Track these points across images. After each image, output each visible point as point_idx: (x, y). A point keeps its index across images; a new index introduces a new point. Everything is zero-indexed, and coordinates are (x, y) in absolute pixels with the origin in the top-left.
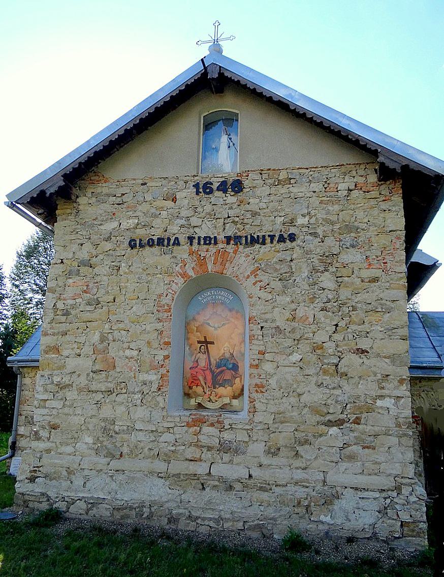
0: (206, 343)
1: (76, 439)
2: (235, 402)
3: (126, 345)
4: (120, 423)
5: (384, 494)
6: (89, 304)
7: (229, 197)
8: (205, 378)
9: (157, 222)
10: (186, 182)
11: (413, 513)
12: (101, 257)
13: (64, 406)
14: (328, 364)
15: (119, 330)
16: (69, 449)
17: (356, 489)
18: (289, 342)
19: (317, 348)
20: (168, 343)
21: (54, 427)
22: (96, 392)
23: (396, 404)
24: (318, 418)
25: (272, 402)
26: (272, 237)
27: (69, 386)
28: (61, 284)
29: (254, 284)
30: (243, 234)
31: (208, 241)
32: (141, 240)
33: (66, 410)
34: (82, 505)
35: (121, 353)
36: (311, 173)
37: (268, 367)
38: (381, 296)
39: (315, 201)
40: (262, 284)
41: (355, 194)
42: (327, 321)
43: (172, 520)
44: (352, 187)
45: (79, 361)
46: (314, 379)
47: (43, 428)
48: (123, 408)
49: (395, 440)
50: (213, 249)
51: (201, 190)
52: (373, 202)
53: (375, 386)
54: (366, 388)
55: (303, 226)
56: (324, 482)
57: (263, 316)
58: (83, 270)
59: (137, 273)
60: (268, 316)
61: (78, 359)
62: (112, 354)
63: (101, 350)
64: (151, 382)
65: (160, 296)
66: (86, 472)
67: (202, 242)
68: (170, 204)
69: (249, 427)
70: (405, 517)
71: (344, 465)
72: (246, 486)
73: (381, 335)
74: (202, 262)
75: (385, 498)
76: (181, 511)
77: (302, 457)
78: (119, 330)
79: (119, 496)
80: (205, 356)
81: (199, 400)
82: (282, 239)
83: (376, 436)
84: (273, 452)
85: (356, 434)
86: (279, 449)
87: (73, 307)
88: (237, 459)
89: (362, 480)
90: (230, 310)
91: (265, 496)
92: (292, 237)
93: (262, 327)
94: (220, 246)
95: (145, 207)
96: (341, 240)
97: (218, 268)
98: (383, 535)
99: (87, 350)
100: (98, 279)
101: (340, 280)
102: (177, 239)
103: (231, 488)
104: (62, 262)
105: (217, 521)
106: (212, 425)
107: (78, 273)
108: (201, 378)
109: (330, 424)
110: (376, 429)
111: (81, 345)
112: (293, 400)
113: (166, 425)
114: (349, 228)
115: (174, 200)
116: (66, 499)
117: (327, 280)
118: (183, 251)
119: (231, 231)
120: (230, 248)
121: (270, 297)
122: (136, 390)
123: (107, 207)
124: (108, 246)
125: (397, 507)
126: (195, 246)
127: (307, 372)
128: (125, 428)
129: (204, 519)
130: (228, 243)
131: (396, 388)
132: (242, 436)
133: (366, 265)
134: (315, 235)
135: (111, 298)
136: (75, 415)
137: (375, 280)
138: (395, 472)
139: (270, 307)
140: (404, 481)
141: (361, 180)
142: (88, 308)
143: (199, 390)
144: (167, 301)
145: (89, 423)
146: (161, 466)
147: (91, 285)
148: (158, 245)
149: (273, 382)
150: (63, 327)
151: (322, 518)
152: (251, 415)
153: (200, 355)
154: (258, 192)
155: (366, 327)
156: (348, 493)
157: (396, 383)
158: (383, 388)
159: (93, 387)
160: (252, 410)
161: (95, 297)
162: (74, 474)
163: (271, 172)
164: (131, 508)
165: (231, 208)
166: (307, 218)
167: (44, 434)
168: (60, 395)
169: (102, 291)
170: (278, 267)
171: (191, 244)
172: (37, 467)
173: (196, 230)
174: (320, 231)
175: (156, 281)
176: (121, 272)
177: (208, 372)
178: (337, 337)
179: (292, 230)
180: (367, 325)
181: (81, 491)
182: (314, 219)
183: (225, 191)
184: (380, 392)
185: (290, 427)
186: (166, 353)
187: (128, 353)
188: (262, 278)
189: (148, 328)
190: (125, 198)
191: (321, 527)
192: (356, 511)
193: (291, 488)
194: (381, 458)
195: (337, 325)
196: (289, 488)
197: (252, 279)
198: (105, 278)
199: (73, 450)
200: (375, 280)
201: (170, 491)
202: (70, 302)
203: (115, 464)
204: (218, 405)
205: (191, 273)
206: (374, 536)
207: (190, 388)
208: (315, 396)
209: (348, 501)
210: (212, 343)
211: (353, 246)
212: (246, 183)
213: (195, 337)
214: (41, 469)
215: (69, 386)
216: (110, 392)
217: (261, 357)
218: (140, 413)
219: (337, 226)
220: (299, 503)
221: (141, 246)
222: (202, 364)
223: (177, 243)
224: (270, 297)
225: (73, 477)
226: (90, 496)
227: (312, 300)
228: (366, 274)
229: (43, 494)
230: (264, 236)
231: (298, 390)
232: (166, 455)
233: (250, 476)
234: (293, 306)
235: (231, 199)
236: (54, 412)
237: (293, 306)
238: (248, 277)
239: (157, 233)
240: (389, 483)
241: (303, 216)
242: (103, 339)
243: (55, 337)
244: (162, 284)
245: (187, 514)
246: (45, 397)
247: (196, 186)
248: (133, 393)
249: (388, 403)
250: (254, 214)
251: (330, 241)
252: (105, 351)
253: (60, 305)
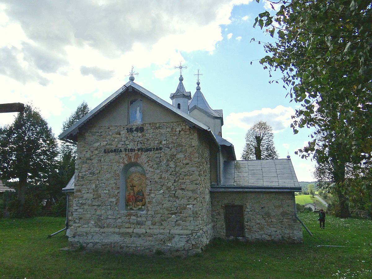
0: (133, 186)
1: (89, 223)
2: (143, 207)
3: (104, 189)
4: (103, 216)
5: (188, 236)
6: (90, 174)
7: (139, 133)
8: (133, 199)
9: (114, 143)
10: (124, 127)
11: (196, 241)
12: (94, 156)
13: (84, 211)
14: (172, 194)
15: (101, 183)
16: (86, 226)
17: (179, 235)
18: (160, 186)
19: (168, 188)
20: (118, 188)
21: (81, 218)
22: (94, 206)
23: (193, 207)
24: (169, 212)
25: (153, 207)
26: (154, 148)
27: (85, 204)
28: (80, 167)
29: (148, 166)
30: (144, 147)
31: (132, 150)
32: (108, 150)
33: (84, 212)
34: (91, 244)
35: (103, 192)
36: (167, 124)
37: (153, 195)
38: (189, 170)
39: (168, 135)
40: (151, 166)
41: (182, 132)
42: (172, 179)
43: (122, 248)
44: (181, 130)
45: (88, 195)
46: (167, 199)
47: (77, 219)
48: (104, 211)
49: (192, 218)
50: (133, 153)
51: (129, 131)
52: (188, 136)
53: (186, 201)
54: (184, 201)
55: (164, 144)
56: (169, 233)
57: (151, 177)
58: (88, 161)
59: (107, 162)
60: (153, 177)
61: (88, 194)
62: (100, 191)
63: (96, 190)
64: (113, 202)
65: (115, 170)
66: (92, 234)
67: (130, 151)
68: (118, 136)
69: (146, 216)
70: (194, 243)
71: (176, 227)
72: (145, 236)
73: (189, 183)
74: (130, 158)
75: (188, 237)
76: (124, 245)
77: (163, 225)
78: (101, 183)
79: (104, 241)
80: (133, 191)
81: (131, 207)
82: (157, 149)
83: (186, 217)
84: (154, 224)
85: (180, 217)
86: (156, 223)
87: (85, 175)
88: (143, 227)
89: (182, 232)
90: (141, 174)
91: (151, 238)
92: (161, 149)
93: (151, 181)
94: (136, 152)
95: (109, 137)
96: (177, 150)
97: (135, 160)
98: (187, 249)
99: (91, 191)
100: (93, 165)
101: (176, 164)
102: (121, 149)
103: (140, 236)
104: (80, 158)
105: (136, 247)
106: (134, 216)
107: (86, 163)
108: (131, 199)
109: (172, 214)
110: (186, 215)
111: (88, 189)
112: (160, 206)
113: (119, 216)
114: (180, 145)
115: (120, 134)
116: (86, 243)
117: (172, 165)
118: (123, 155)
119: (140, 146)
120: (139, 153)
121: (153, 170)
122: (108, 204)
123: (95, 137)
124: (96, 152)
125: (192, 240)
126: (127, 153)
127: (165, 196)
128: (105, 218)
129: (132, 247)
130: (139, 151)
131: (193, 201)
132: (144, 219)
133: (185, 159)
134: (168, 148)
135: (98, 171)
136: (88, 214)
137: (187, 164)
138: (192, 229)
139: (153, 174)
140: (194, 231)
141: (184, 127)
142: (91, 175)
143: (131, 203)
144: (119, 173)
145: (92, 217)
146: (117, 230)
147: (91, 167)
148: (114, 152)
149: (154, 200)
150: (82, 183)
151: (168, 244)
152: (147, 212)
153: (131, 191)
154: (149, 131)
155: (184, 181)
156: (177, 236)
157: (193, 200)
158: (189, 201)
159: (94, 203)
160: (147, 210)
161: (93, 171)
162: (88, 234)
163: (154, 124)
164: (108, 245)
165: (139, 138)
166: (166, 141)
167: (77, 221)
168: (82, 207)
169: (95, 169)
170: (156, 159)
171: (126, 152)
172: (76, 232)
173: (128, 146)
174: (170, 146)
175: (114, 165)
176: (102, 162)
177: (133, 197)
178: (175, 184)
179: (161, 146)
180: (184, 180)
181: (91, 240)
182: (168, 142)
183: (137, 132)
184: (188, 203)
185: (160, 215)
186: (118, 191)
187: (105, 191)
188: (151, 164)
189: (112, 182)
190: (102, 134)
191: (168, 247)
192: (179, 242)
193: (159, 236)
194: (188, 224)
195: (175, 180)
196: (158, 235)
197: (147, 164)
198: (96, 164)
199: (88, 226)
200: (187, 164)
201: (120, 238)
202: (84, 173)
203: (102, 230)
204: (137, 208)
205: (126, 162)
206: (184, 249)
207: (128, 203)
208: (167, 204)
209: (177, 239)
210: (135, 186)
211: (181, 152)
212: (145, 128)
213: (129, 184)
214: (77, 233)
215: (85, 204)
216: (99, 206)
217: (150, 192)
218: (110, 212)
219: (175, 145)
220: (161, 240)
221: (109, 152)
222: (132, 194)
223: (121, 151)
224: (153, 170)
225: (88, 235)
226: (94, 241)
227: (167, 171)
228: (185, 162)
229: (78, 241)
230: (151, 148)
231: (162, 203)
232: (119, 226)
233: (146, 232)
234: (161, 173)
235: (140, 134)
236: (80, 213)
237: (161, 173)
238: (146, 163)
239: (113, 147)
240: (189, 232)
241: (165, 140)
242: (96, 187)
243: (79, 187)
244: (116, 166)
245: (126, 245)
246: (77, 208)
247: (127, 129)
248: (108, 206)
249: (191, 206)
250: (148, 140)
251: (173, 150)
252: (97, 191)
253: (80, 175)
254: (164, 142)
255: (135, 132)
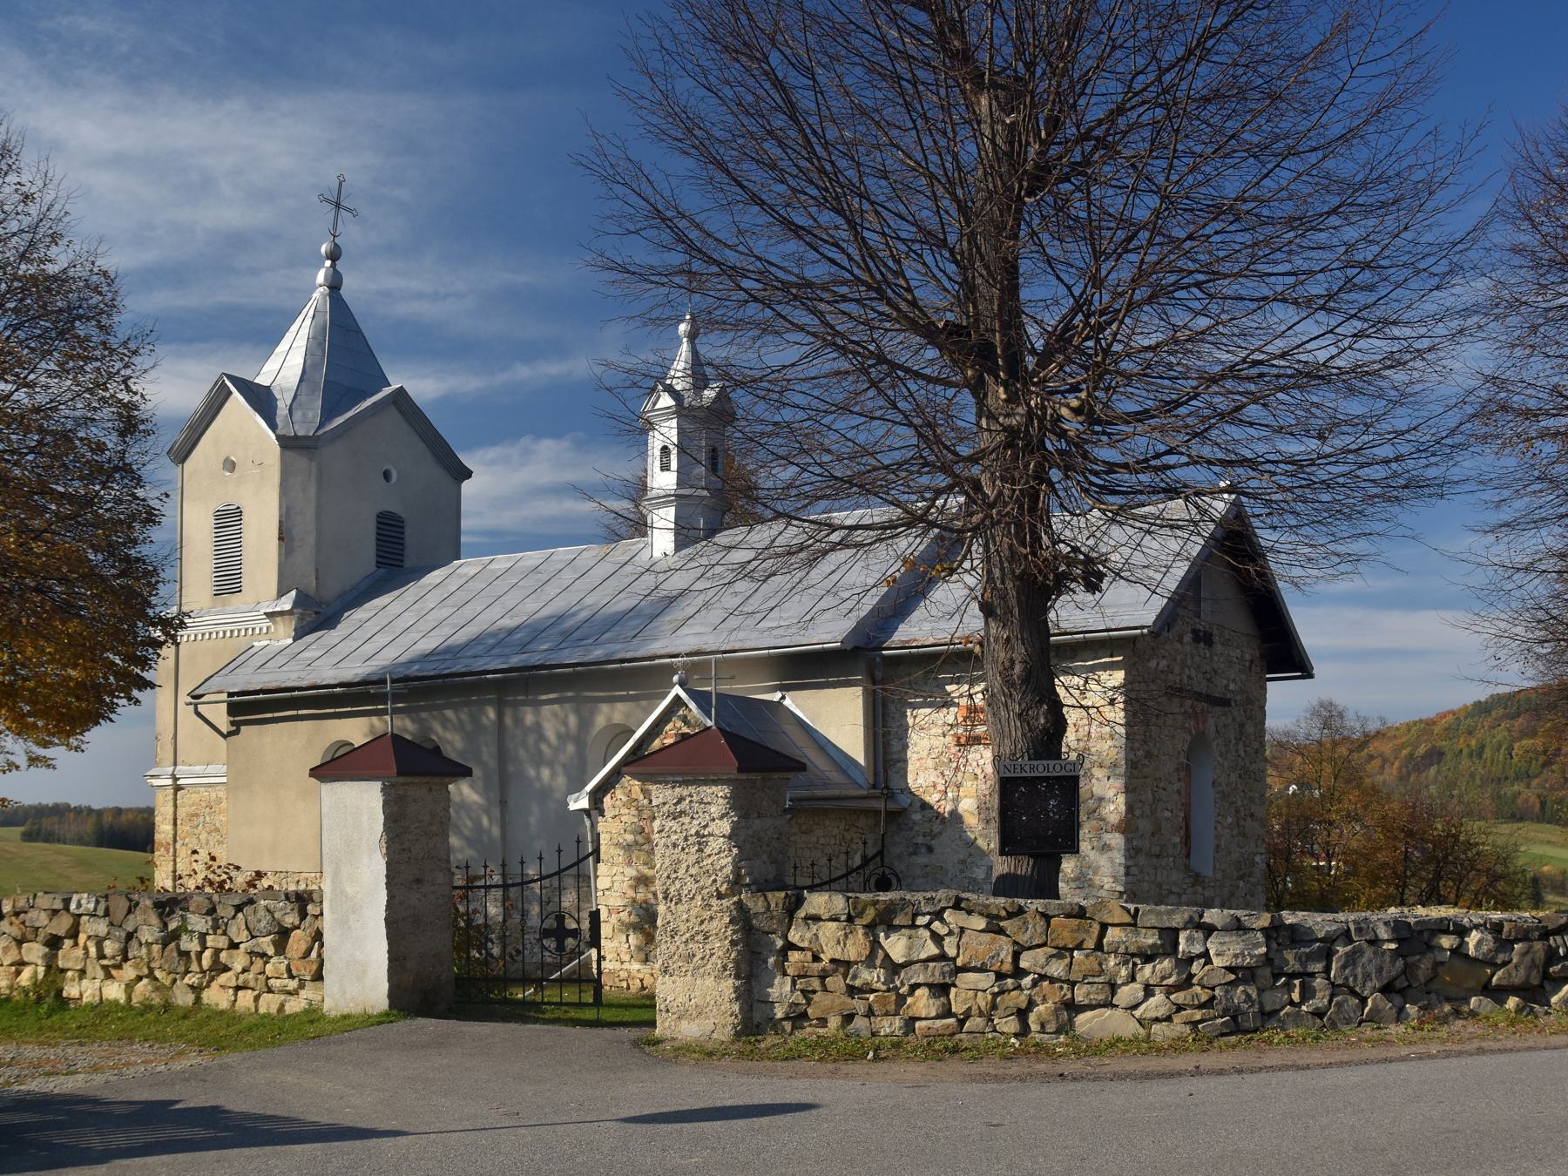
37: (1219, 828)
68: (1178, 645)
99: (1147, 810)
109: (1241, 878)
174: (1238, 698)
254: (1232, 686)
255: (1202, 645)
